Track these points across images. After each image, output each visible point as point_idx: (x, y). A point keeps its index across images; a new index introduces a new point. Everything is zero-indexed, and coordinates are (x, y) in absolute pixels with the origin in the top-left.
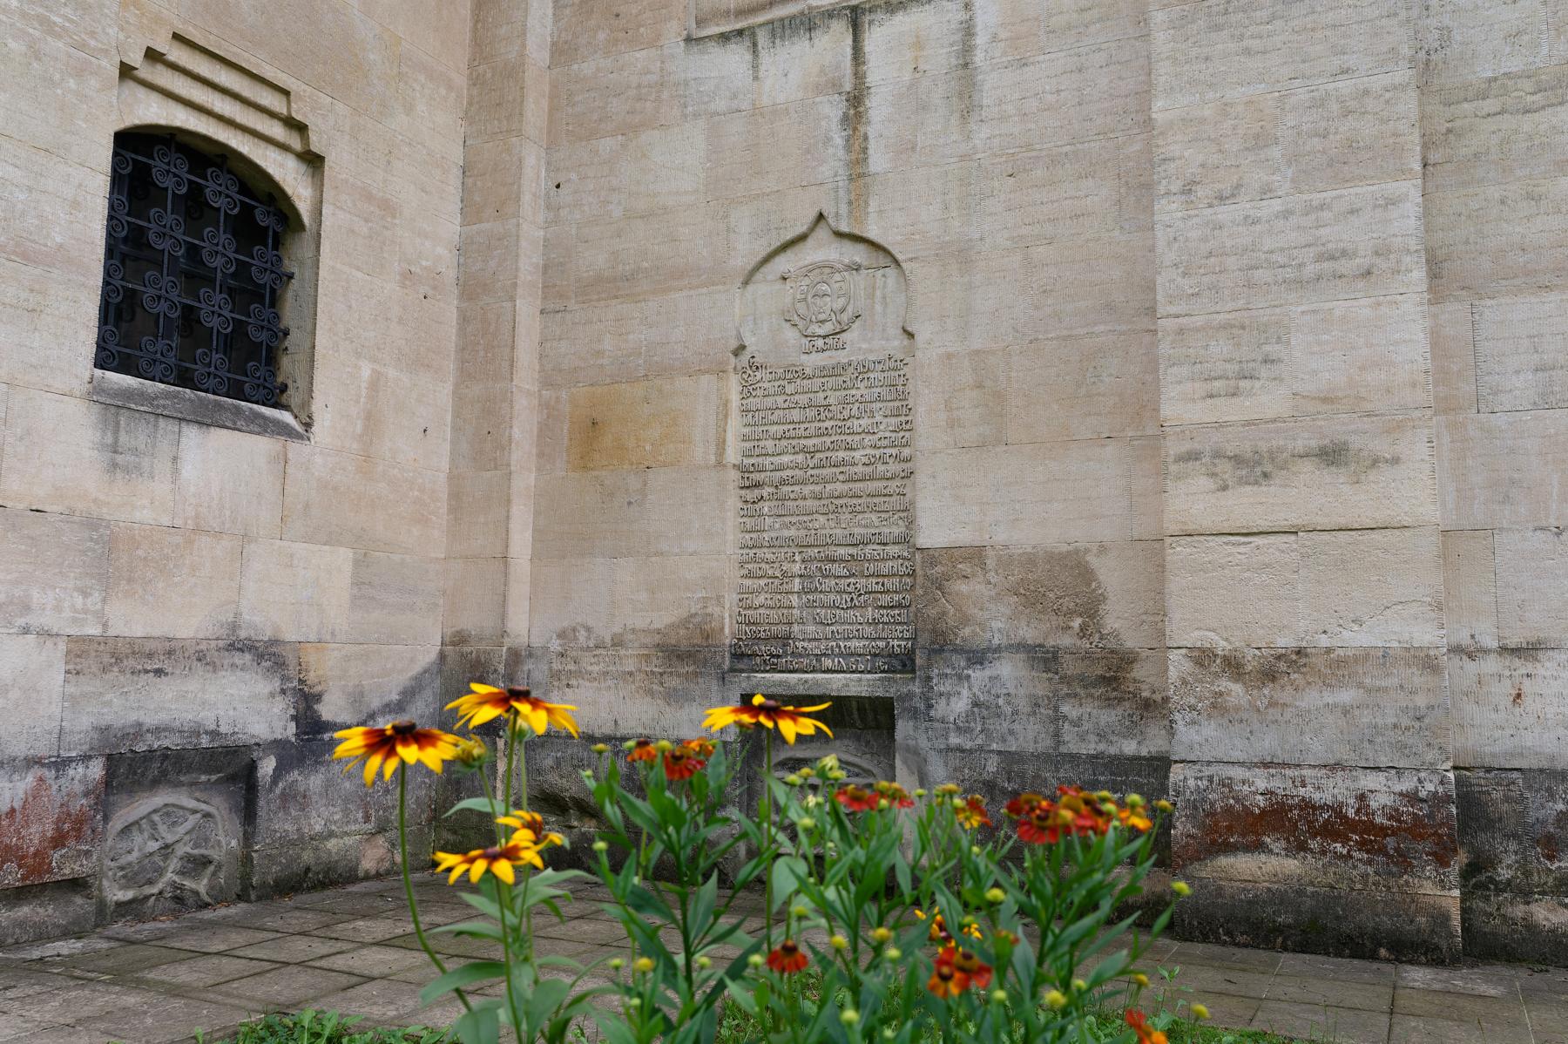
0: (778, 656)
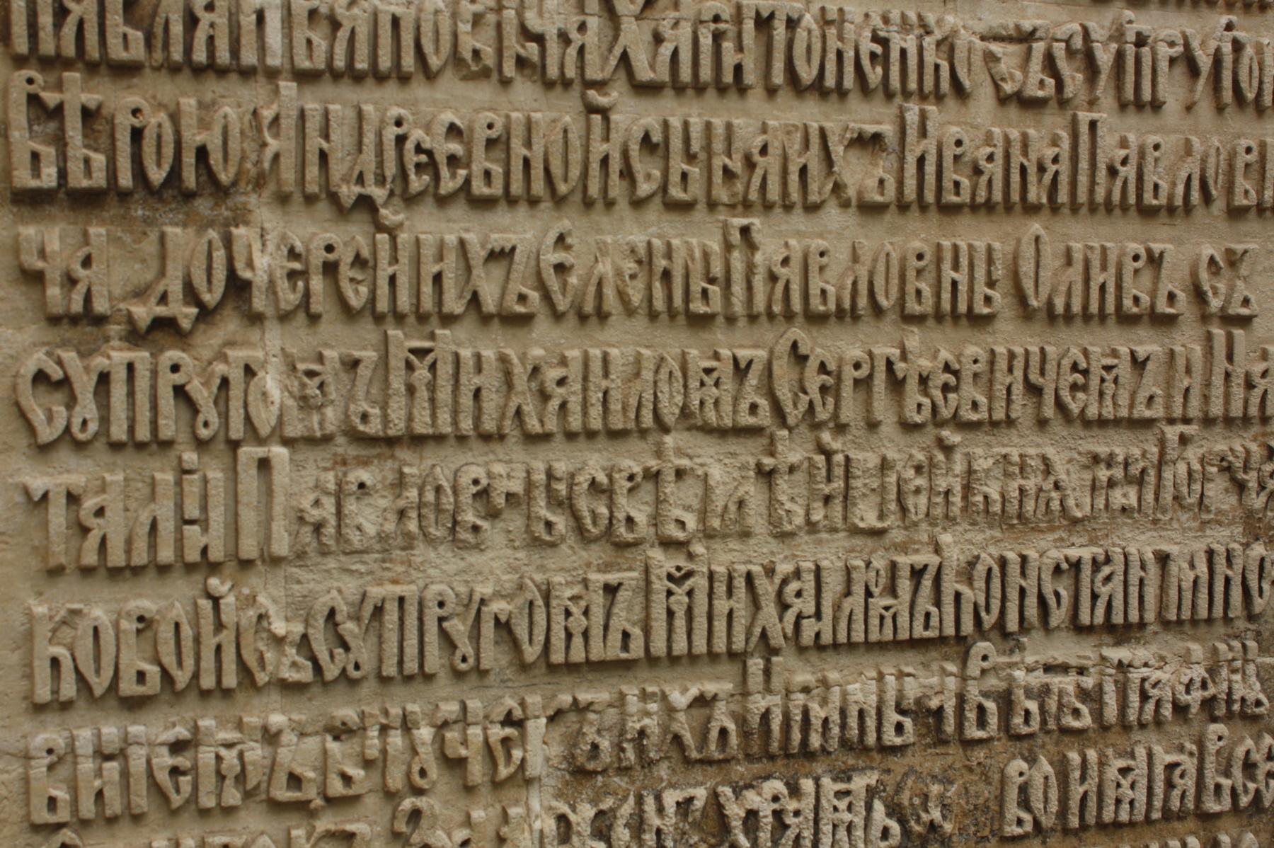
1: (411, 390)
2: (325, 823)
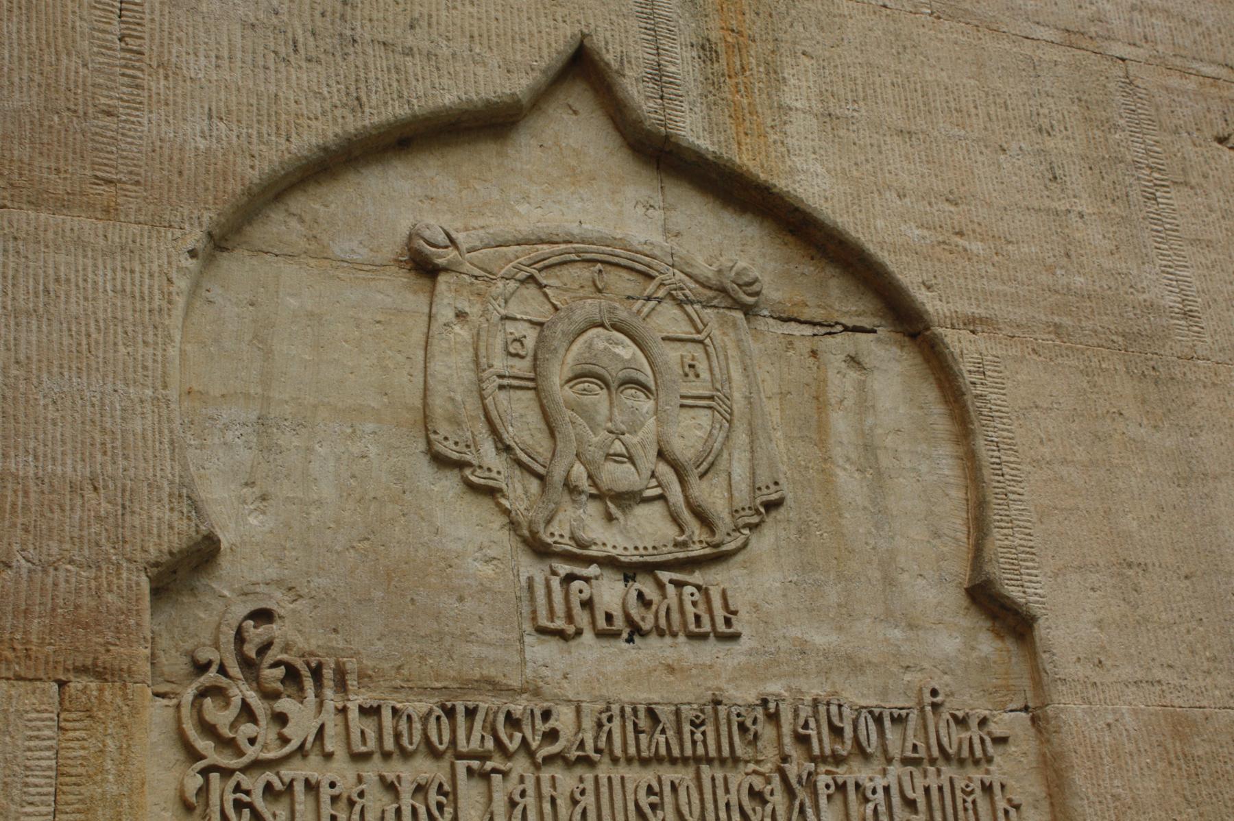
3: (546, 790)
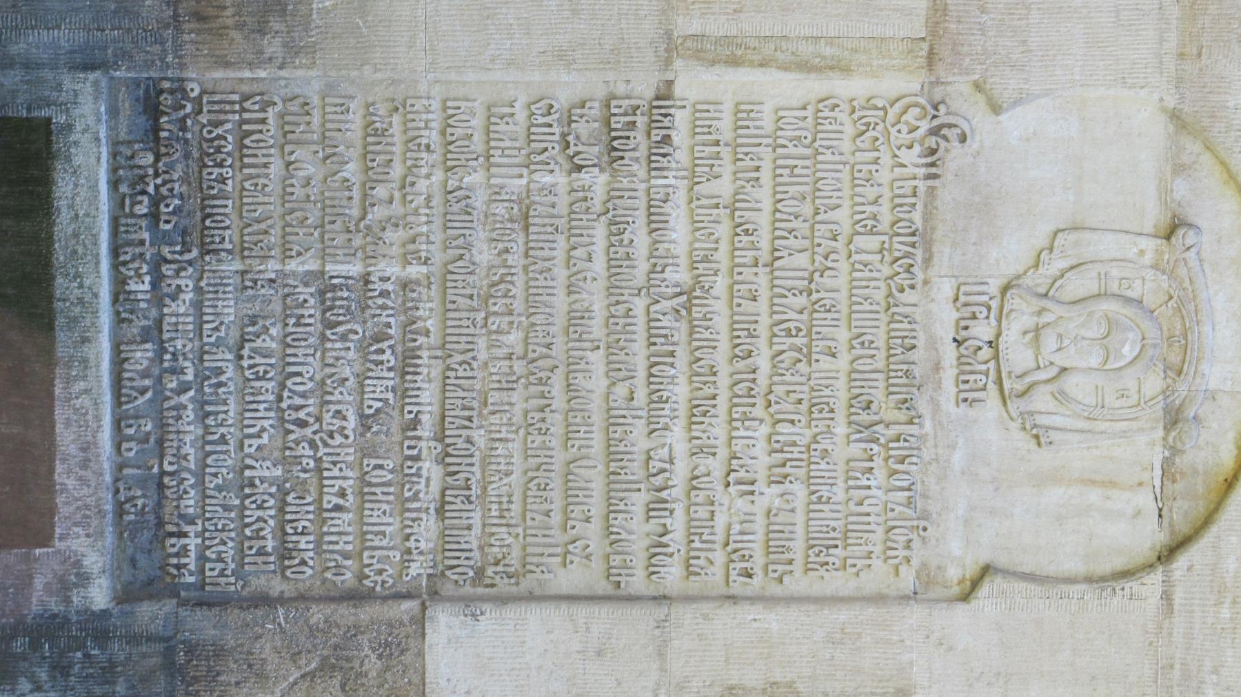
0: (154, 216)
1: (544, 226)
2: (397, 195)
3: (873, 284)
